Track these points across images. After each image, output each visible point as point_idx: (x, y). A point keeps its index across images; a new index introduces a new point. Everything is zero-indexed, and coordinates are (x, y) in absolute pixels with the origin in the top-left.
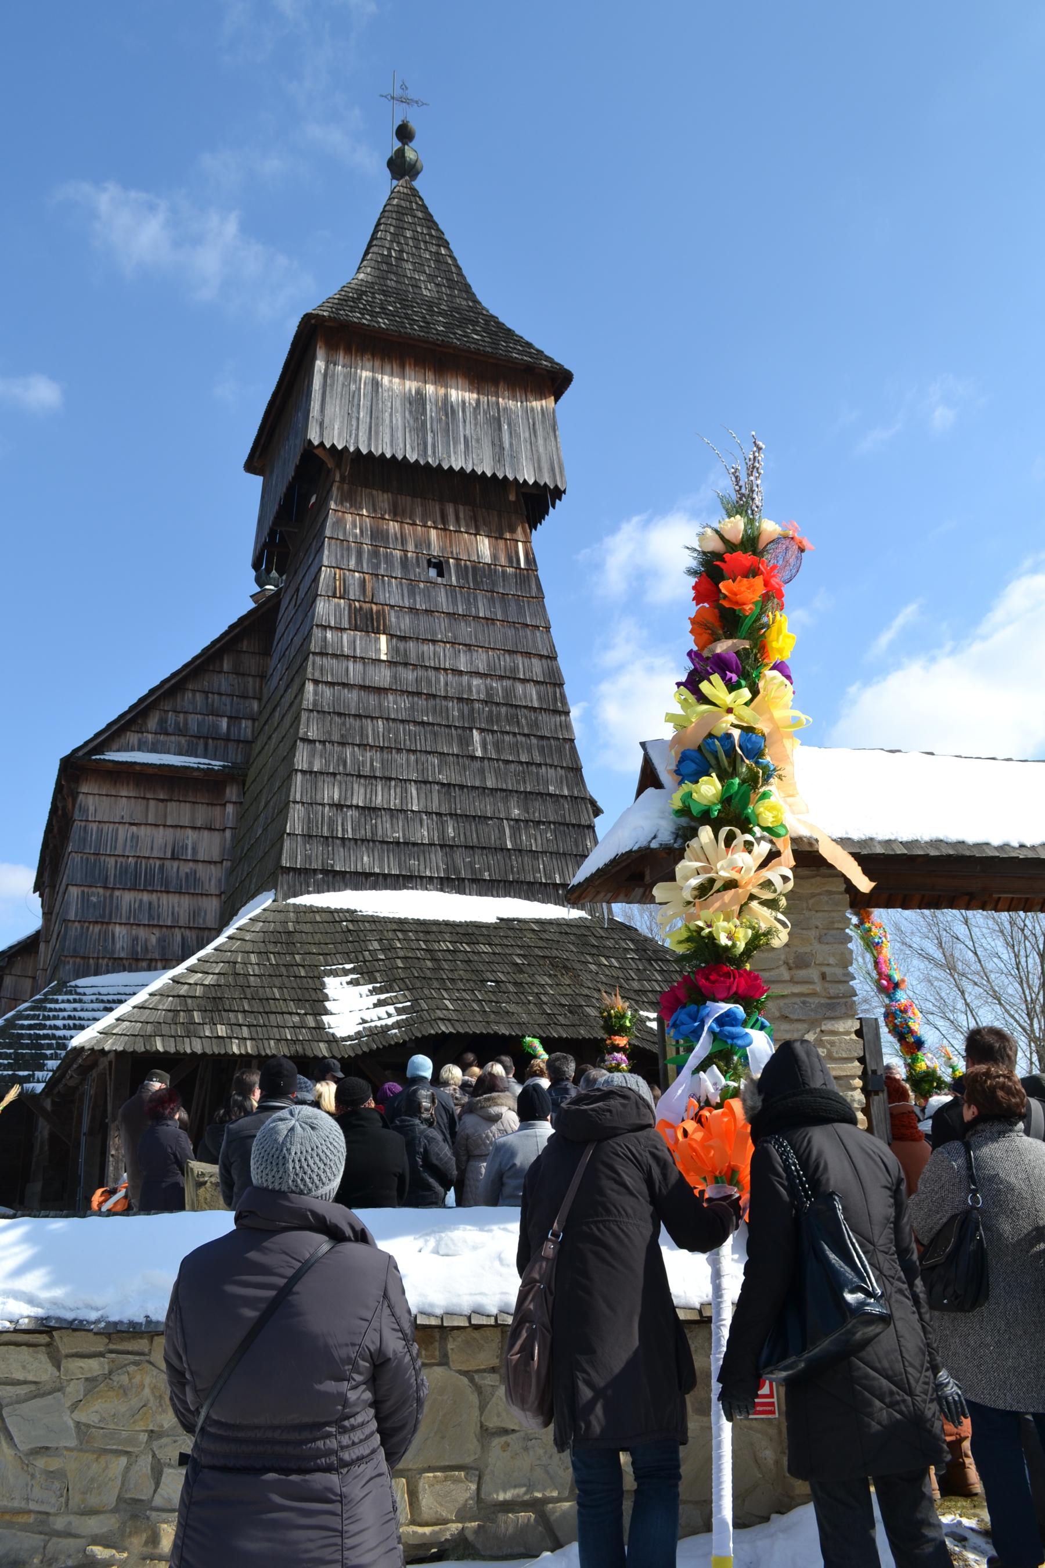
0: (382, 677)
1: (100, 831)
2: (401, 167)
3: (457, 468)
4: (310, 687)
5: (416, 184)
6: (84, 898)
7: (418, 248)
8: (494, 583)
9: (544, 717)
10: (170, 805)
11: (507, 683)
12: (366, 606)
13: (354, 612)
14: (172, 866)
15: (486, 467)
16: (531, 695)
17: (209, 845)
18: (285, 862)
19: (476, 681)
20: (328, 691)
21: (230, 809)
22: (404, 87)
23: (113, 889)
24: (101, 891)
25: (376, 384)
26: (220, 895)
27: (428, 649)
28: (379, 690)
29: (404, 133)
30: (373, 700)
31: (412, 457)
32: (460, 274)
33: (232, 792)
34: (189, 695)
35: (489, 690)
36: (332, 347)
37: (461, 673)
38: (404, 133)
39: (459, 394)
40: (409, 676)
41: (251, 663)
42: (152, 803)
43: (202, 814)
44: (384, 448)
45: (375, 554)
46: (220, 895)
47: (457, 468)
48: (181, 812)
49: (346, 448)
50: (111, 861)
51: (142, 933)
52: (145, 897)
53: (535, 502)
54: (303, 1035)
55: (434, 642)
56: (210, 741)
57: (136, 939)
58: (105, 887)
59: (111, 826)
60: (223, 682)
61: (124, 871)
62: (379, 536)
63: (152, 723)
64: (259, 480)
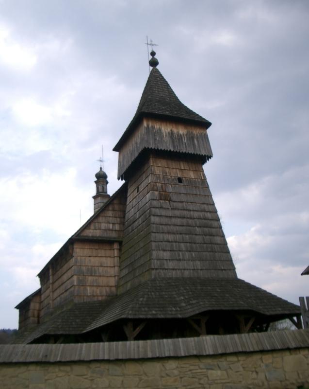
1: (81, 259)
2: (154, 63)
3: (184, 152)
5: (158, 67)
6: (78, 279)
7: (162, 87)
10: (99, 250)
11: (203, 213)
12: (164, 193)
13: (160, 195)
14: (101, 269)
16: (209, 215)
17: (109, 262)
21: (116, 250)
22: (151, 41)
23: (86, 276)
24: (82, 276)
26: (115, 276)
28: (170, 217)
29: (153, 54)
31: (172, 150)
33: (116, 246)
34: (101, 218)
38: (153, 54)
40: (177, 213)
41: (116, 207)
42: (94, 250)
43: (108, 253)
47: (184, 152)
48: (102, 252)
49: (154, 148)
50: (84, 268)
51: (95, 289)
52: (95, 278)
53: (203, 159)
55: (182, 202)
56: (108, 231)
58: (84, 275)
59: (84, 258)
60: (110, 213)
64: (117, 153)
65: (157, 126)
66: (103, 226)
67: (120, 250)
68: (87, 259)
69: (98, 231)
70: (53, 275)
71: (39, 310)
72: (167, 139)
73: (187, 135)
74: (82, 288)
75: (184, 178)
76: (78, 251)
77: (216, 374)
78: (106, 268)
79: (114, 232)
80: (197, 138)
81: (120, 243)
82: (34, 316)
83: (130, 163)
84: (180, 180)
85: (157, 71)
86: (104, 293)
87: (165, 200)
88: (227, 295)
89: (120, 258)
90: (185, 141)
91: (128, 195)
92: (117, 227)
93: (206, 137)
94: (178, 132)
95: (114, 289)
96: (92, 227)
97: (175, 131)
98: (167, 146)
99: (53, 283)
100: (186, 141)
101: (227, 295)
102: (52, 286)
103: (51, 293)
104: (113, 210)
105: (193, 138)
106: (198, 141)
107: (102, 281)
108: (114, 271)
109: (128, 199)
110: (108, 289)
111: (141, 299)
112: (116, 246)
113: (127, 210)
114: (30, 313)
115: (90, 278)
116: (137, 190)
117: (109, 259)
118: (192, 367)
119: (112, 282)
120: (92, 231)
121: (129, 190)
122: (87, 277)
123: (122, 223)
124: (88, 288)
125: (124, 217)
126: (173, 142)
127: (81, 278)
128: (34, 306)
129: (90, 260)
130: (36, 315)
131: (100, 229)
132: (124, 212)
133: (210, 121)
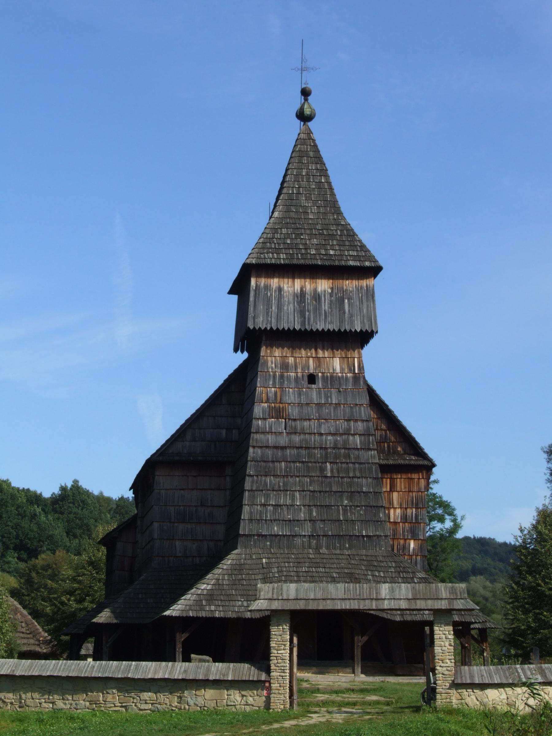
0: (283, 440)
3: (320, 329)
4: (251, 450)
9: (361, 453)
18: (241, 532)
19: (330, 438)
20: (259, 451)
23: (174, 523)
25: (280, 289)
27: (306, 424)
28: (283, 448)
29: (305, 93)
30: (280, 453)
36: (258, 276)
37: (321, 434)
38: (305, 93)
39: (323, 285)
40: (297, 439)
44: (285, 325)
47: (320, 329)
50: (172, 509)
52: (189, 526)
53: (363, 338)
55: (310, 420)
58: (170, 522)
65: (275, 282)
72: (290, 308)
73: (331, 295)
75: (320, 374)
76: (163, 481)
84: (312, 379)
85: (309, 133)
87: (277, 418)
90: (325, 306)
93: (370, 294)
94: (315, 290)
96: (189, 436)
98: (291, 321)
100: (326, 308)
105: (341, 301)
115: (181, 527)
120: (187, 444)
122: (176, 524)
124: (178, 543)
127: (165, 527)
133: (381, 263)
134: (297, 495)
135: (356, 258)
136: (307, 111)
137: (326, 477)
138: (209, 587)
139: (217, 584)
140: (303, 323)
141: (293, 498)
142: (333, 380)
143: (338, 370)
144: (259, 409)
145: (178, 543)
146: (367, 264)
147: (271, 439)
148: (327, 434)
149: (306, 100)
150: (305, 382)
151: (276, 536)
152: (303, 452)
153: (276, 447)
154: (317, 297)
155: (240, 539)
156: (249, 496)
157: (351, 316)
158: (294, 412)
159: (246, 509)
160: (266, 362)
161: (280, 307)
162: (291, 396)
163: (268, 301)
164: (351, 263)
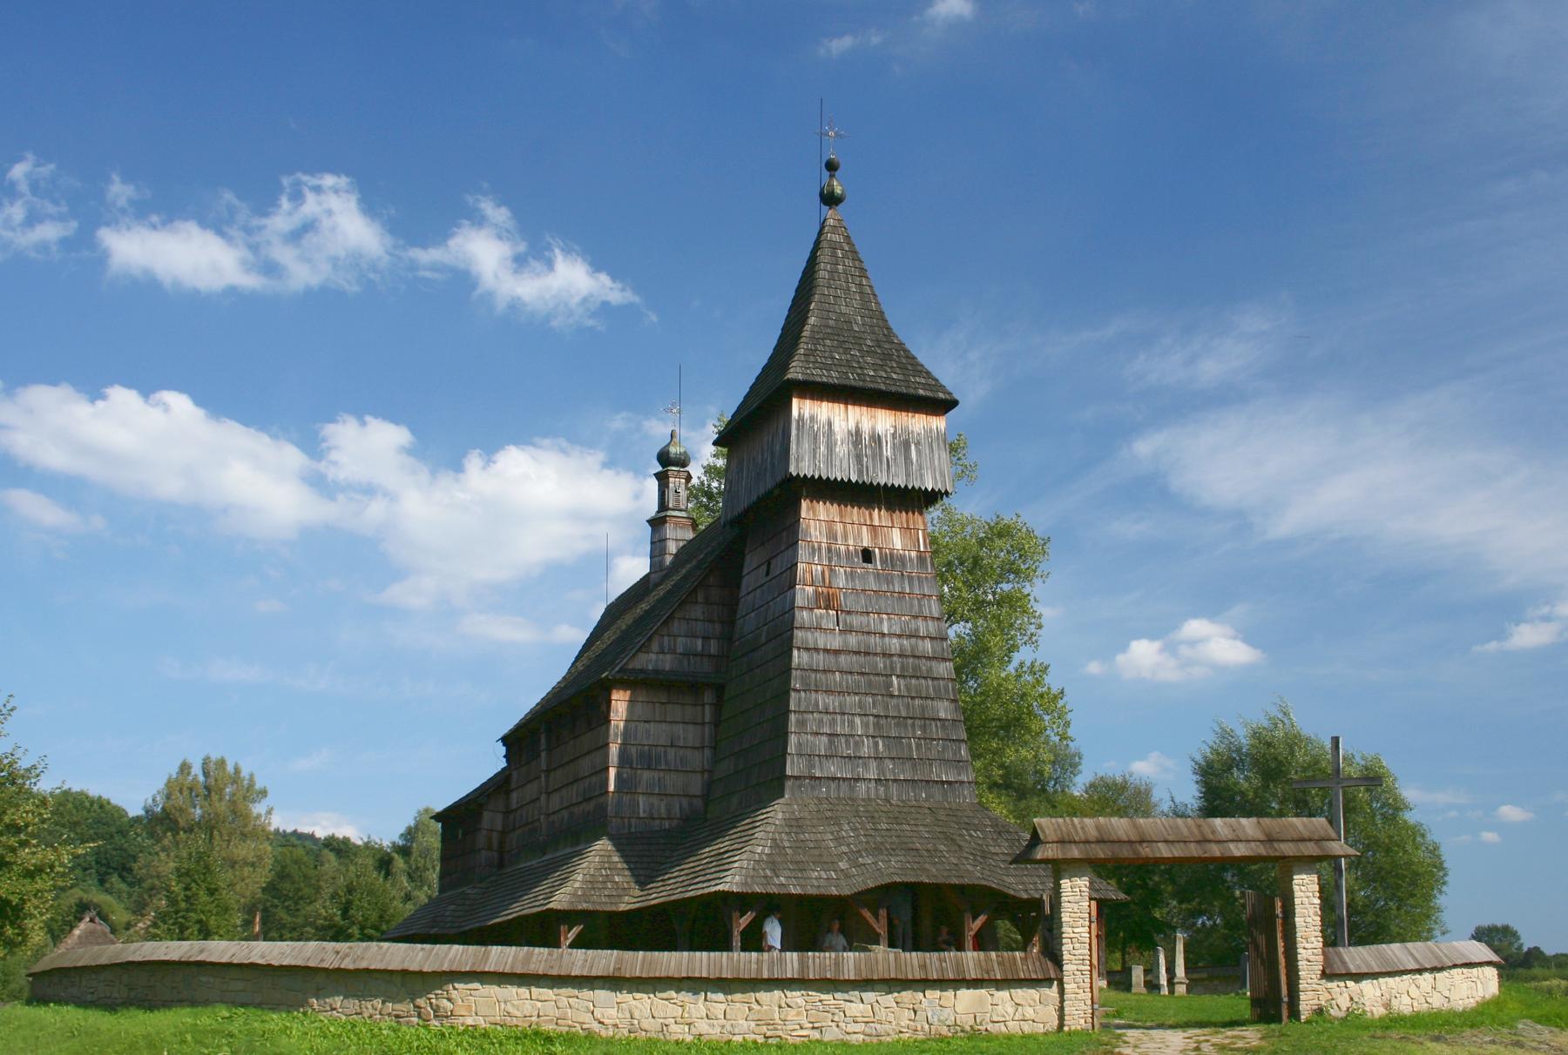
0: (835, 642)
4: (795, 653)
8: (904, 565)
10: (669, 707)
14: (671, 752)
15: (899, 481)
18: (789, 772)
19: (895, 640)
26: (702, 772)
27: (864, 619)
28: (837, 652)
29: (831, 167)
30: (832, 658)
32: (877, 303)
34: (676, 623)
35: (901, 646)
37: (883, 635)
40: (853, 640)
44: (838, 474)
45: (829, 550)
46: (702, 772)
48: (675, 711)
51: (655, 800)
52: (656, 775)
54: (823, 883)
57: (652, 805)
60: (697, 611)
61: (641, 755)
62: (832, 535)
63: (655, 646)
66: (681, 643)
67: (718, 707)
68: (642, 726)
69: (668, 657)
70: (549, 750)
71: (503, 833)
72: (842, 450)
73: (894, 435)
74: (626, 798)
77: (856, 1009)
78: (681, 752)
79: (705, 660)
80: (918, 444)
81: (720, 689)
82: (490, 848)
83: (754, 498)
84: (867, 555)
86: (676, 811)
88: (942, 847)
89: (716, 726)
90: (888, 451)
91: (745, 571)
92: (713, 647)
94: (873, 429)
95: (698, 803)
97: (866, 427)
98: (843, 469)
99: (548, 771)
101: (942, 847)
102: (547, 777)
103: (543, 797)
104: (707, 602)
105: (906, 444)
106: (919, 452)
107: (673, 781)
108: (697, 760)
109: (744, 581)
110: (685, 802)
111: (759, 850)
112: (708, 697)
113: (742, 609)
114: (481, 839)
115: (646, 775)
116: (764, 567)
117: (691, 727)
118: (823, 997)
119: (696, 785)
121: (748, 558)
123: (728, 638)
125: (732, 623)
126: (859, 458)
128: (491, 819)
129: (648, 731)
130: (495, 845)
131: (673, 652)
132: (731, 605)
134: (858, 720)
135: (925, 386)
136: (838, 190)
137: (892, 696)
138: (767, 851)
139: (776, 845)
140: (860, 472)
141: (852, 724)
142: (892, 560)
143: (898, 546)
144: (804, 593)
145: (641, 799)
146: (941, 395)
147: (822, 641)
148: (890, 635)
149: (832, 176)
150: (858, 560)
151: (834, 779)
152: (862, 659)
153: (826, 651)
154: (876, 439)
155: (789, 784)
156: (798, 721)
157: (921, 468)
158: (849, 603)
159: (793, 739)
160: (807, 533)
161: (831, 447)
162: (841, 582)
163: (815, 437)
164: (921, 392)
